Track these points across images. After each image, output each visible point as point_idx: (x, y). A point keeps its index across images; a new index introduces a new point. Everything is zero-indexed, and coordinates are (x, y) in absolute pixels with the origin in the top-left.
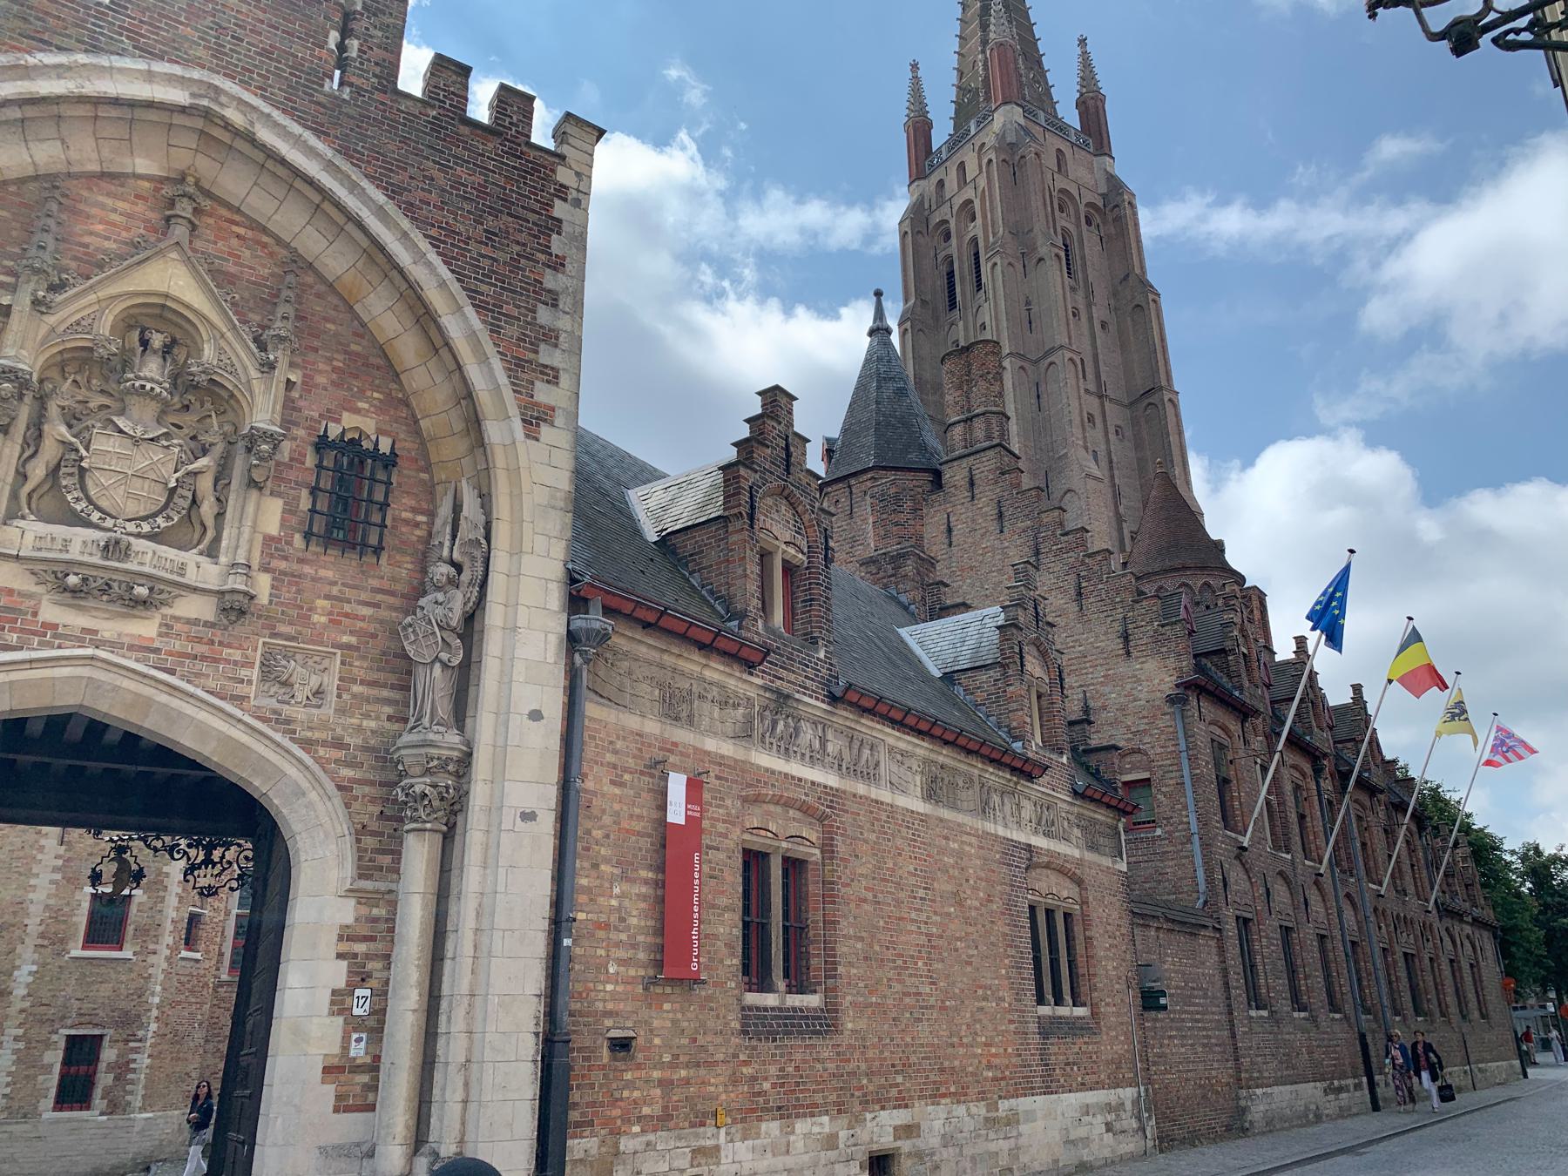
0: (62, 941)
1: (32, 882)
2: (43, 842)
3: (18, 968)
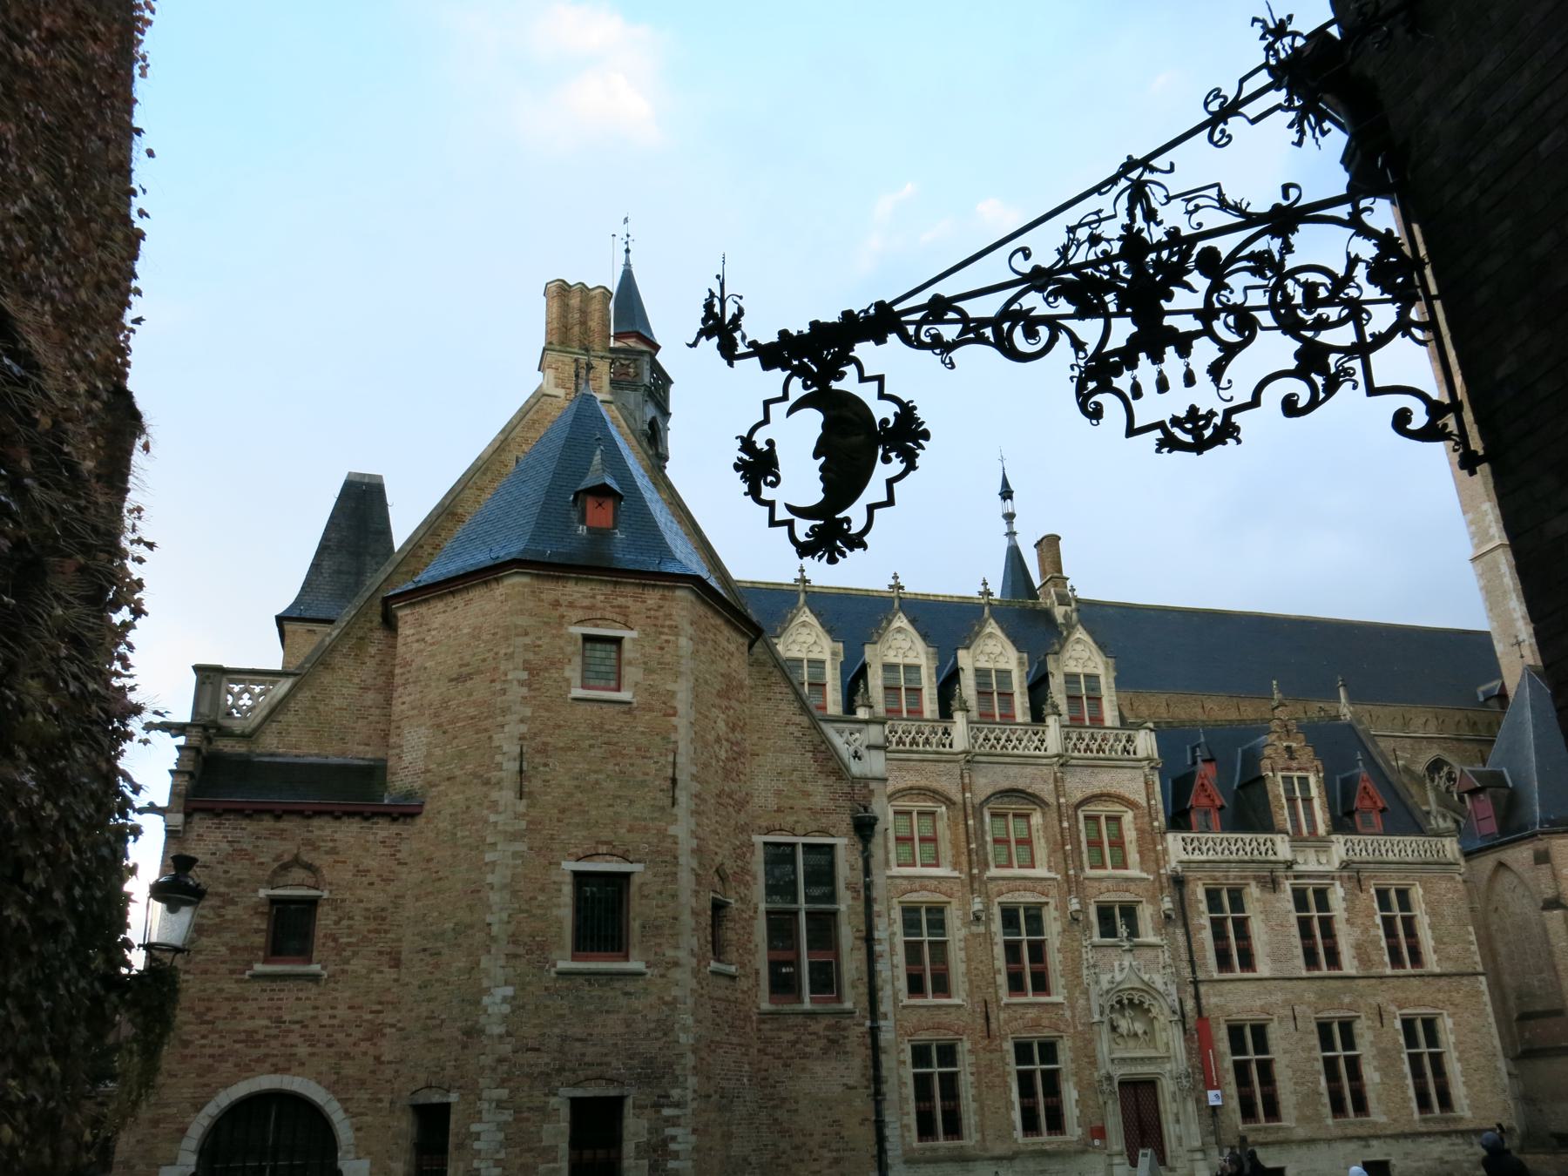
0: (542, 947)
1: (489, 857)
2: (495, 795)
3: (487, 991)
